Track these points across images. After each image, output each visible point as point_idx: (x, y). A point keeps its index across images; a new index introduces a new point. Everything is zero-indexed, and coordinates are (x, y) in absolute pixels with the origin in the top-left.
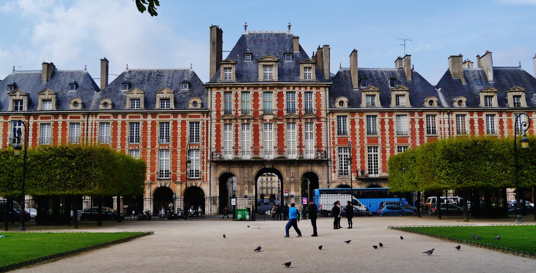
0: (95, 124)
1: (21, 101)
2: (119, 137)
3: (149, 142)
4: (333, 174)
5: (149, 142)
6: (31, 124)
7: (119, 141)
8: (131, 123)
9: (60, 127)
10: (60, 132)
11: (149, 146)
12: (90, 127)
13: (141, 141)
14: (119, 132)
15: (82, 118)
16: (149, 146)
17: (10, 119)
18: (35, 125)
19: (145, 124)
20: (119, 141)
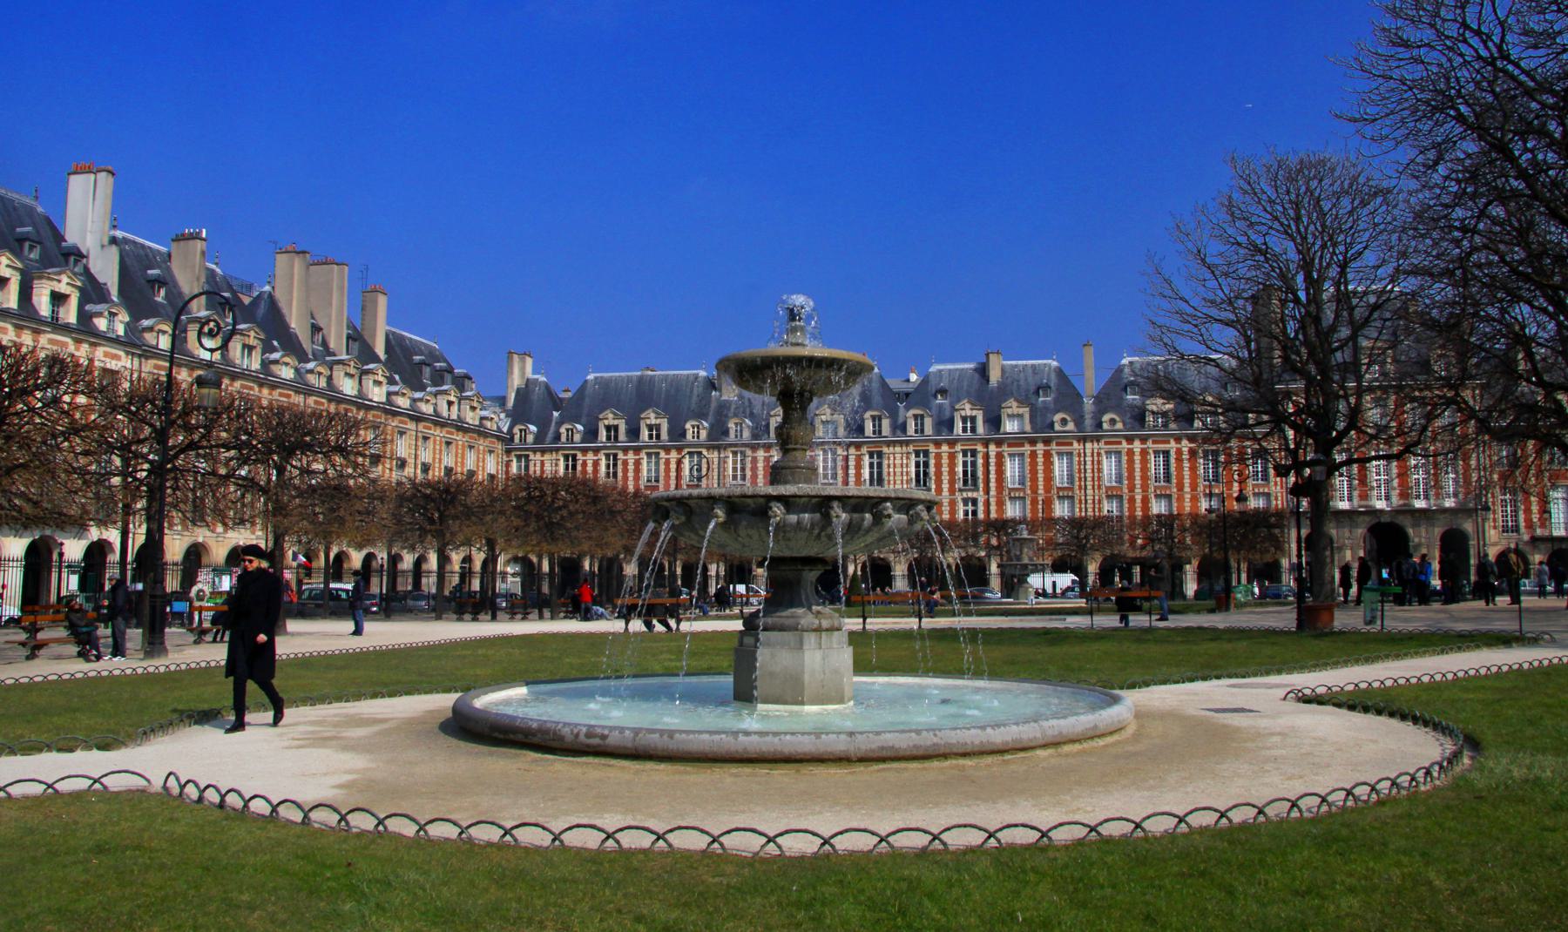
0: (1099, 454)
1: (973, 419)
2: (1138, 474)
3: (1187, 481)
4: (1492, 532)
5: (1187, 481)
6: (992, 454)
7: (1138, 482)
8: (1156, 452)
9: (1040, 460)
10: (1040, 468)
11: (1187, 489)
12: (1089, 459)
13: (1174, 481)
14: (1138, 466)
15: (1076, 445)
16: (1187, 489)
17: (959, 447)
18: (1000, 456)
19: (1179, 452)
20: (1138, 482)
